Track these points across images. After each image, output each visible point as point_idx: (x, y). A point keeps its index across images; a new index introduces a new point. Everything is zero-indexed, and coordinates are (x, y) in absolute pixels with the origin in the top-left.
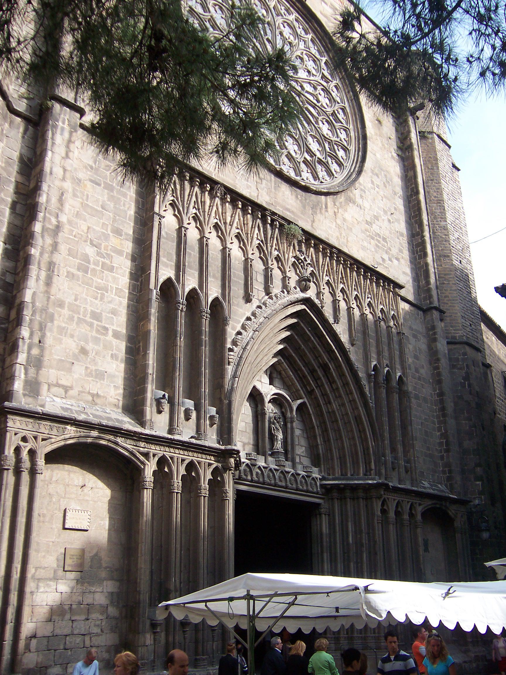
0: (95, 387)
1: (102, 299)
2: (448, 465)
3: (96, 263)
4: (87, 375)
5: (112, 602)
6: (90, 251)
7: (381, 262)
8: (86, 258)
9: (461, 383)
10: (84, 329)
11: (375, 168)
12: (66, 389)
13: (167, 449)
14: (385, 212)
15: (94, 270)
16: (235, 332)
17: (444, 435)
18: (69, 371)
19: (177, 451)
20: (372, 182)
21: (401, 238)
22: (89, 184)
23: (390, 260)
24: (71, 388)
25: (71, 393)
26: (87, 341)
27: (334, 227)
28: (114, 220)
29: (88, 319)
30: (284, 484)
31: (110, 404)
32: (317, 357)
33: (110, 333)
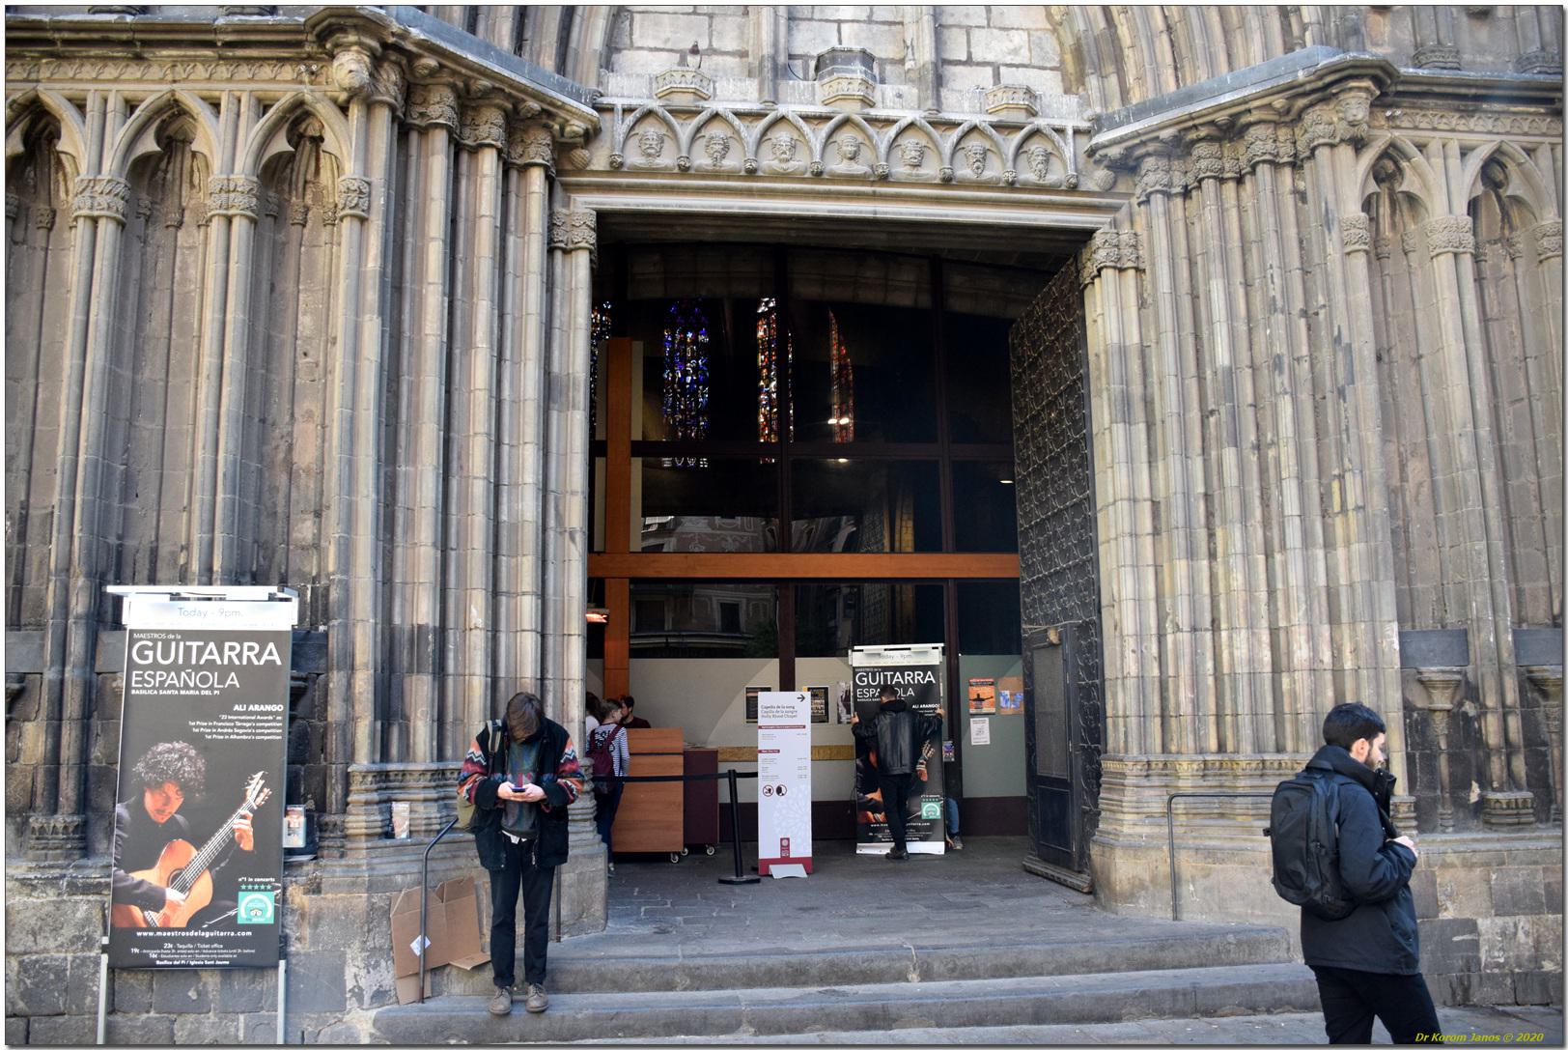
19: (88, 71)
30: (859, 168)
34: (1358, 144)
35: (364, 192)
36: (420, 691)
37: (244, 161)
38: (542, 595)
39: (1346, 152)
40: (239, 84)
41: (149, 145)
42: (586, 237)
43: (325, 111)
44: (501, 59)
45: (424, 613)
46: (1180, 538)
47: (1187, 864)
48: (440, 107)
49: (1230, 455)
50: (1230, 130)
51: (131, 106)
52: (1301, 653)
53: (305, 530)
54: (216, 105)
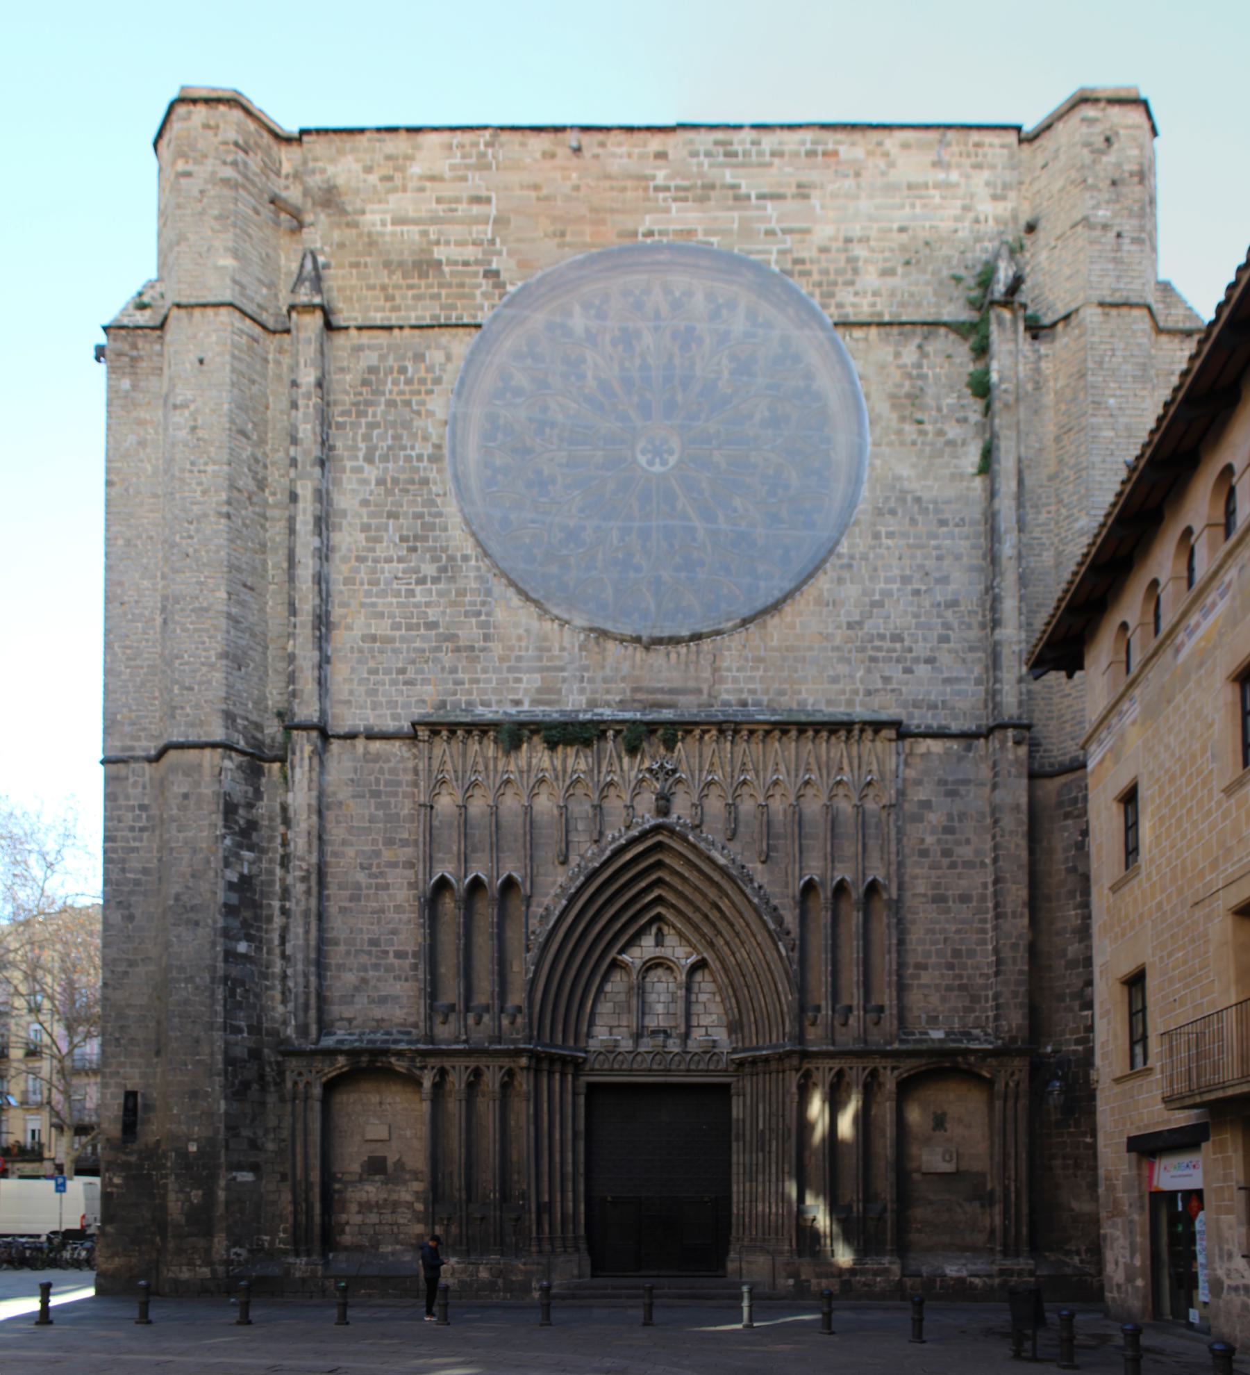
0: (378, 1013)
1: (379, 923)
2: (996, 997)
3: (369, 887)
4: (370, 1003)
5: (418, 1200)
6: (361, 877)
7: (880, 685)
8: (358, 886)
9: (1076, 843)
10: (364, 959)
11: (887, 499)
12: (350, 1021)
13: (445, 1059)
14: (905, 580)
15: (368, 896)
16: (541, 910)
17: (996, 951)
18: (352, 1002)
20: (876, 536)
21: (949, 614)
22: (351, 802)
23: (908, 671)
24: (355, 1018)
25: (355, 1023)
26: (365, 970)
27: (761, 673)
28: (386, 830)
29: (366, 948)
31: (397, 1025)
32: (704, 895)
33: (391, 954)
34: (797, 1070)
35: (529, 1092)
36: (546, 1218)
37: (497, 1085)
38: (575, 1191)
39: (793, 1073)
40: (494, 1063)
41: (472, 1078)
42: (582, 1090)
43: (517, 1070)
44: (562, 1048)
45: (546, 1198)
46: (747, 1177)
47: (744, 1266)
48: (545, 1065)
49: (760, 1155)
50: (766, 1060)
51: (467, 1068)
52: (774, 1210)
53: (515, 1177)
54: (488, 1067)
